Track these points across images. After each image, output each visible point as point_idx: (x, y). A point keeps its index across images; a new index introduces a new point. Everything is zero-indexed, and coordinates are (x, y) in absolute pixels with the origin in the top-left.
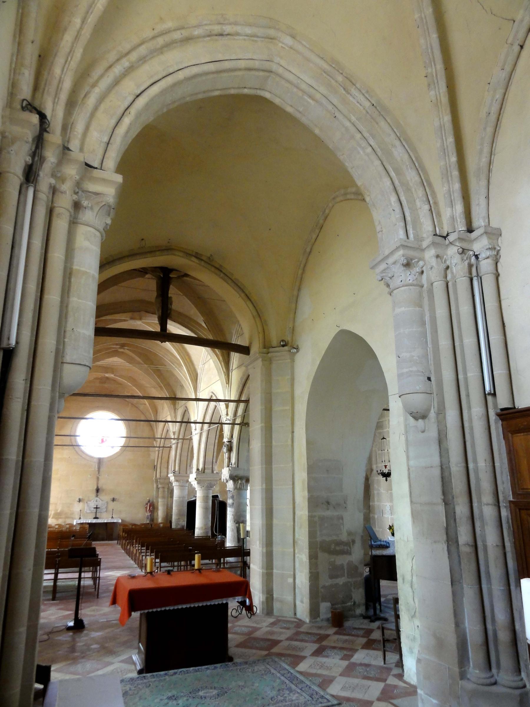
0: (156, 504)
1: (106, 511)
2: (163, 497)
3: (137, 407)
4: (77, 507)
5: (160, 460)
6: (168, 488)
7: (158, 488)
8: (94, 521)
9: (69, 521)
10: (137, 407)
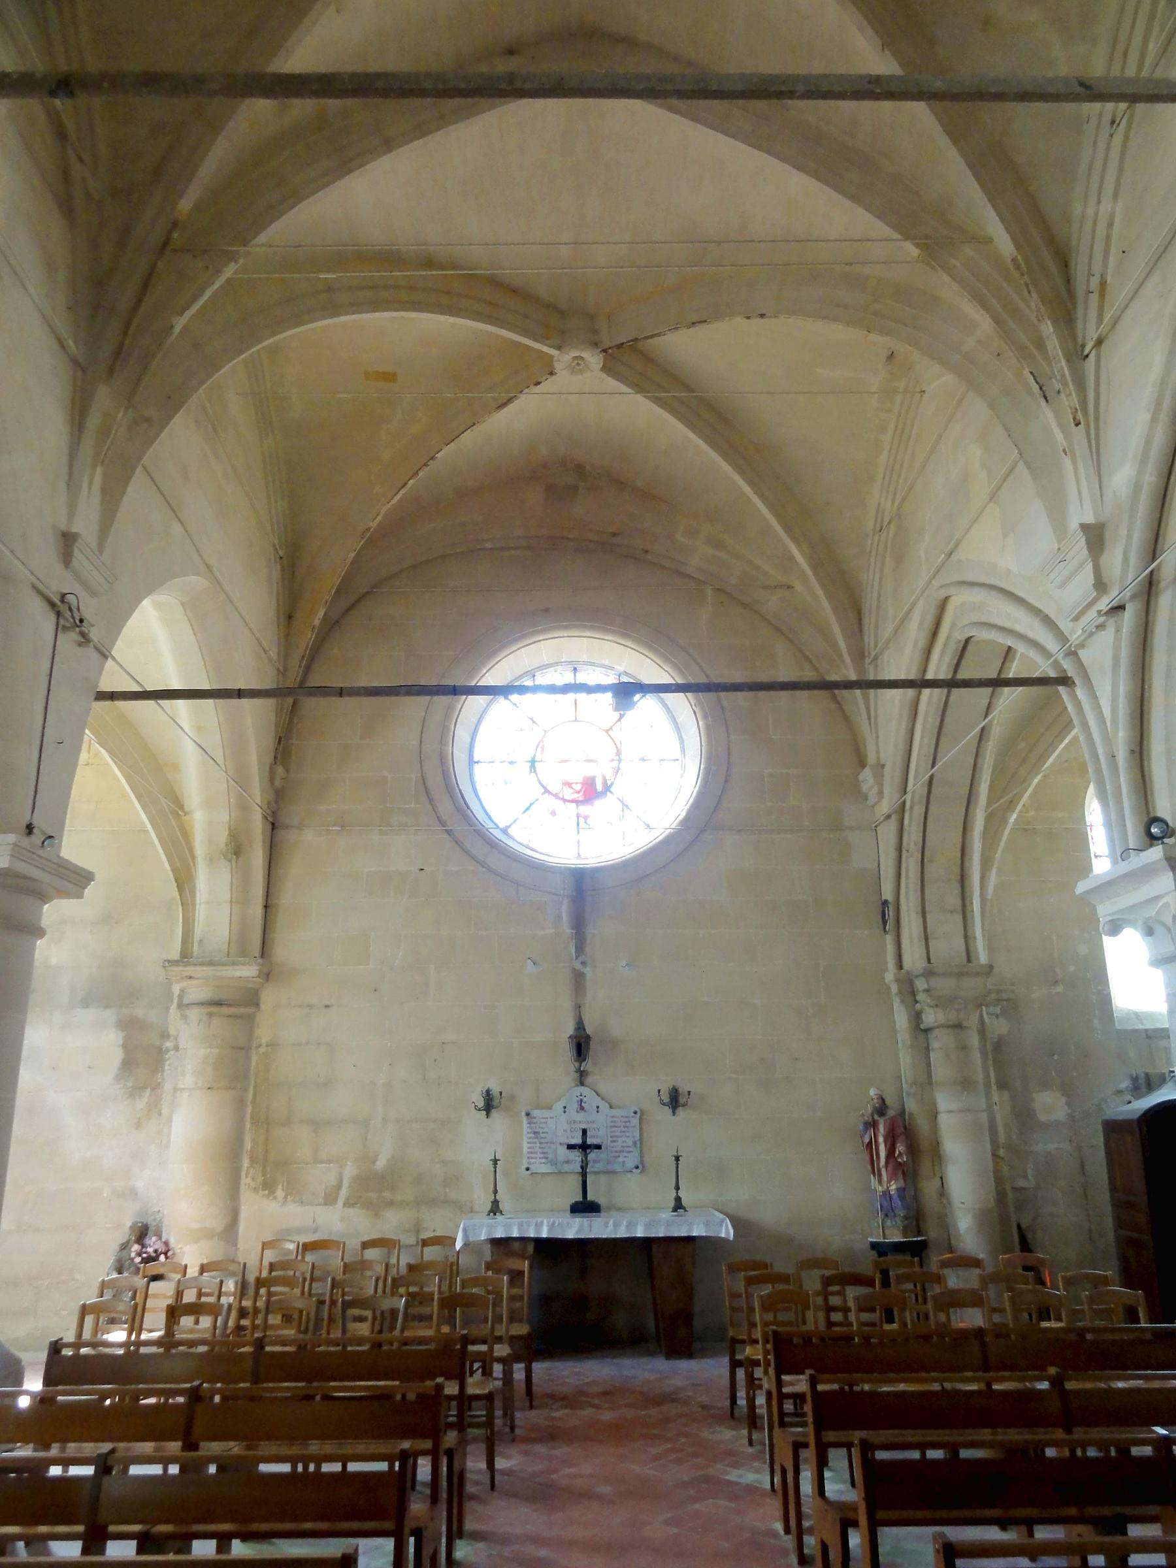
0: (922, 1125)
1: (641, 1167)
2: (965, 1084)
3: (745, 605)
4: (479, 1142)
5: (911, 865)
6: (982, 1031)
7: (920, 1031)
8: (574, 1228)
9: (435, 1223)
10: (745, 605)
